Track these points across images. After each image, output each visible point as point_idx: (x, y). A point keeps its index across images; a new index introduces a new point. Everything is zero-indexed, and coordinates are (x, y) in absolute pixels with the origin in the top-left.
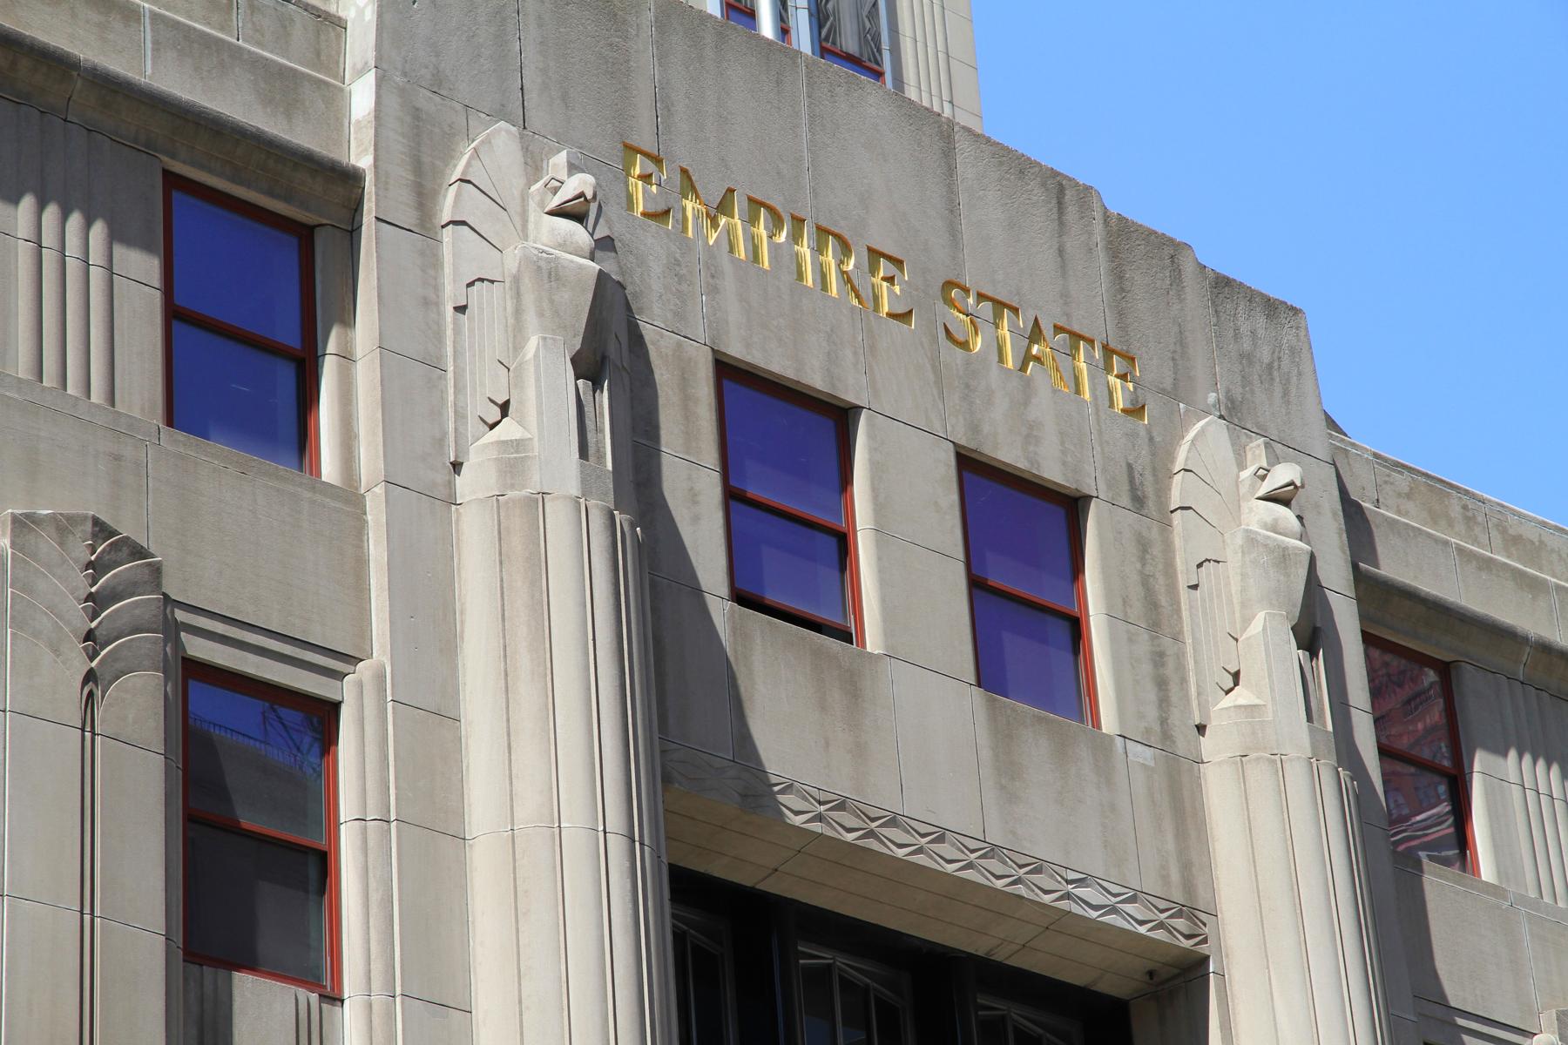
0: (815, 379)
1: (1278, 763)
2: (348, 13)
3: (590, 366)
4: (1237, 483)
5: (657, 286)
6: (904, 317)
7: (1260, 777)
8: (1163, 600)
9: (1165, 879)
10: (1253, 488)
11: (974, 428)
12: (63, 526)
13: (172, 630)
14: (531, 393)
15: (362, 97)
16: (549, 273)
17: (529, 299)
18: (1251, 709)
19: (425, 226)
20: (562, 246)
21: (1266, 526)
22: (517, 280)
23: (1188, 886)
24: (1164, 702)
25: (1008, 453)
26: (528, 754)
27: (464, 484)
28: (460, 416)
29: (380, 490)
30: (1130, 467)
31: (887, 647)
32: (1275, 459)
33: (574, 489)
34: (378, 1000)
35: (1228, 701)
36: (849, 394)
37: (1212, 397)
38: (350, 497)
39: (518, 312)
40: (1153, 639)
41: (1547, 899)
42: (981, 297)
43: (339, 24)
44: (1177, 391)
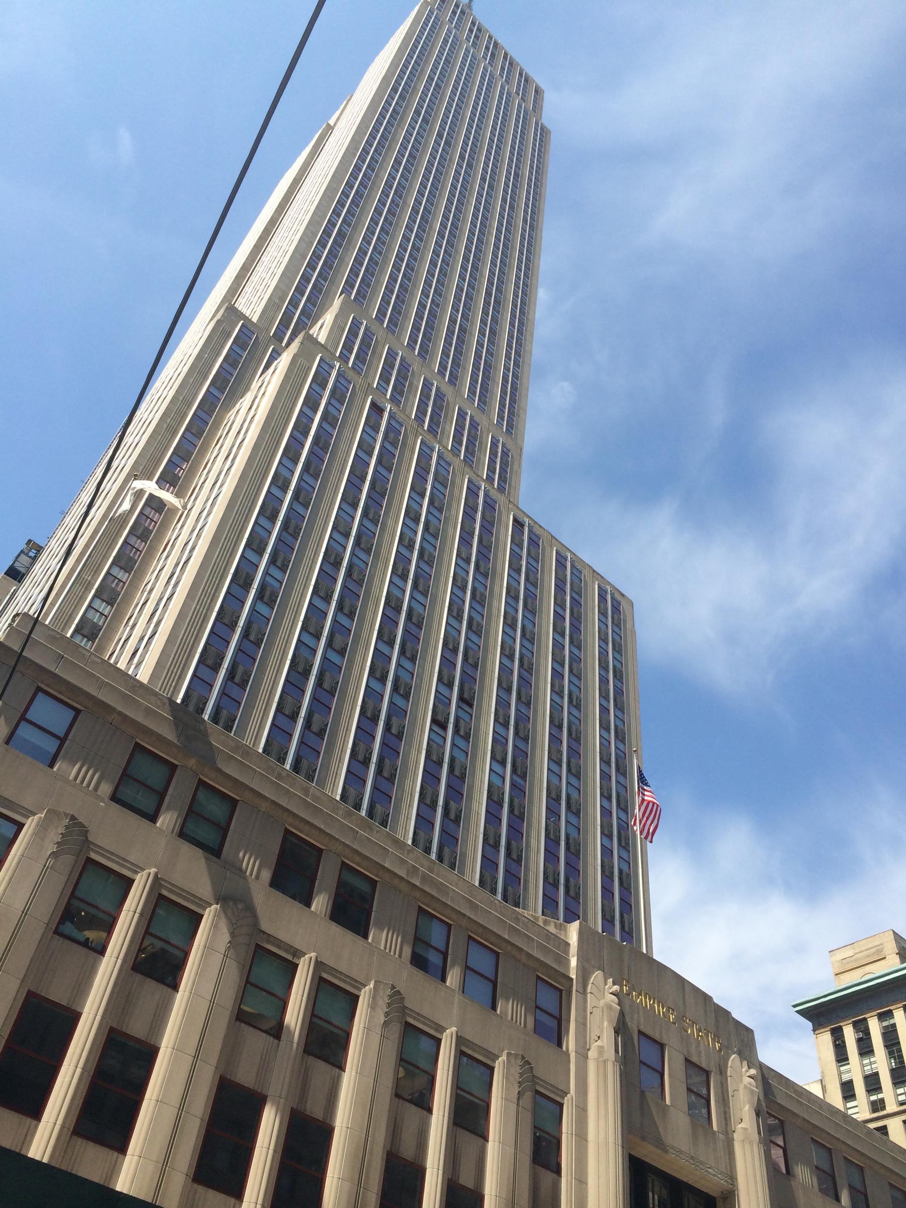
0: (657, 1037)
1: (751, 1143)
2: (571, 943)
3: (617, 1032)
4: (741, 1072)
5: (627, 1011)
6: (675, 1023)
7: (747, 1146)
8: (726, 1098)
9: (727, 1169)
10: (746, 1074)
11: (688, 1051)
12: (516, 1055)
13: (535, 1083)
14: (605, 1035)
15: (573, 962)
16: (610, 1007)
17: (605, 1013)
18: (745, 1129)
19: (584, 992)
20: (612, 1001)
21: (748, 1083)
22: (602, 1008)
23: (731, 1171)
24: (726, 1125)
25: (694, 1059)
26: (602, 1123)
27: (590, 1053)
28: (590, 1038)
29: (574, 1053)
30: (719, 1064)
31: (671, 1103)
32: (749, 1068)
33: (613, 1059)
34: (569, 1178)
35: (740, 1126)
36: (664, 1041)
37: (735, 1049)
38: (567, 1054)
39: (603, 1015)
40: (724, 1108)
41: (805, 1183)
42: (690, 1020)
43: (569, 944)
44: (728, 1047)
